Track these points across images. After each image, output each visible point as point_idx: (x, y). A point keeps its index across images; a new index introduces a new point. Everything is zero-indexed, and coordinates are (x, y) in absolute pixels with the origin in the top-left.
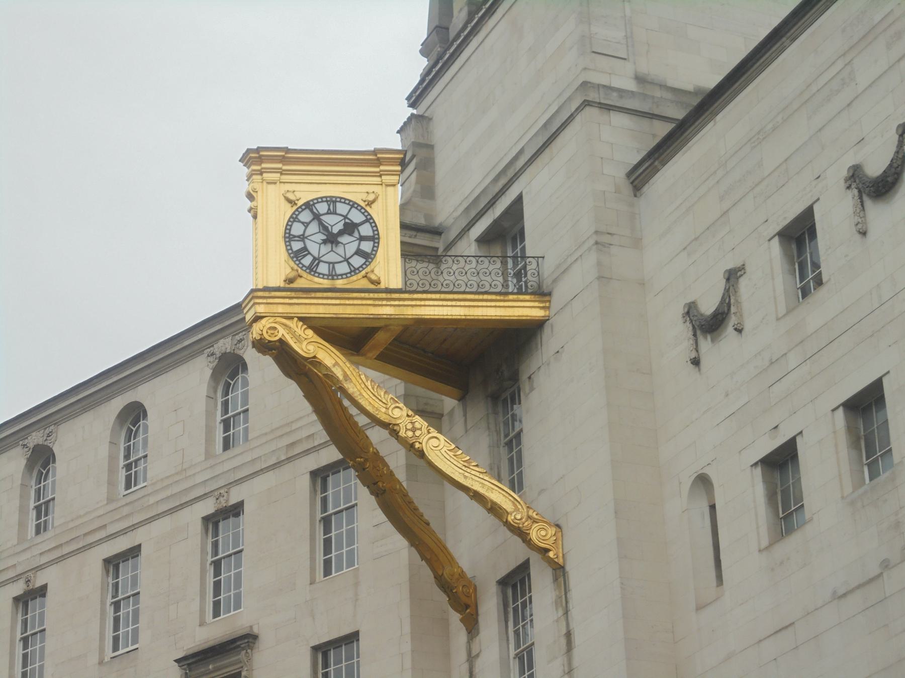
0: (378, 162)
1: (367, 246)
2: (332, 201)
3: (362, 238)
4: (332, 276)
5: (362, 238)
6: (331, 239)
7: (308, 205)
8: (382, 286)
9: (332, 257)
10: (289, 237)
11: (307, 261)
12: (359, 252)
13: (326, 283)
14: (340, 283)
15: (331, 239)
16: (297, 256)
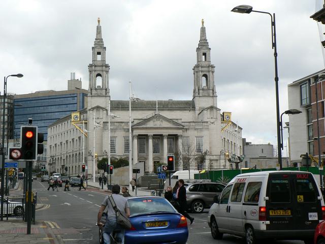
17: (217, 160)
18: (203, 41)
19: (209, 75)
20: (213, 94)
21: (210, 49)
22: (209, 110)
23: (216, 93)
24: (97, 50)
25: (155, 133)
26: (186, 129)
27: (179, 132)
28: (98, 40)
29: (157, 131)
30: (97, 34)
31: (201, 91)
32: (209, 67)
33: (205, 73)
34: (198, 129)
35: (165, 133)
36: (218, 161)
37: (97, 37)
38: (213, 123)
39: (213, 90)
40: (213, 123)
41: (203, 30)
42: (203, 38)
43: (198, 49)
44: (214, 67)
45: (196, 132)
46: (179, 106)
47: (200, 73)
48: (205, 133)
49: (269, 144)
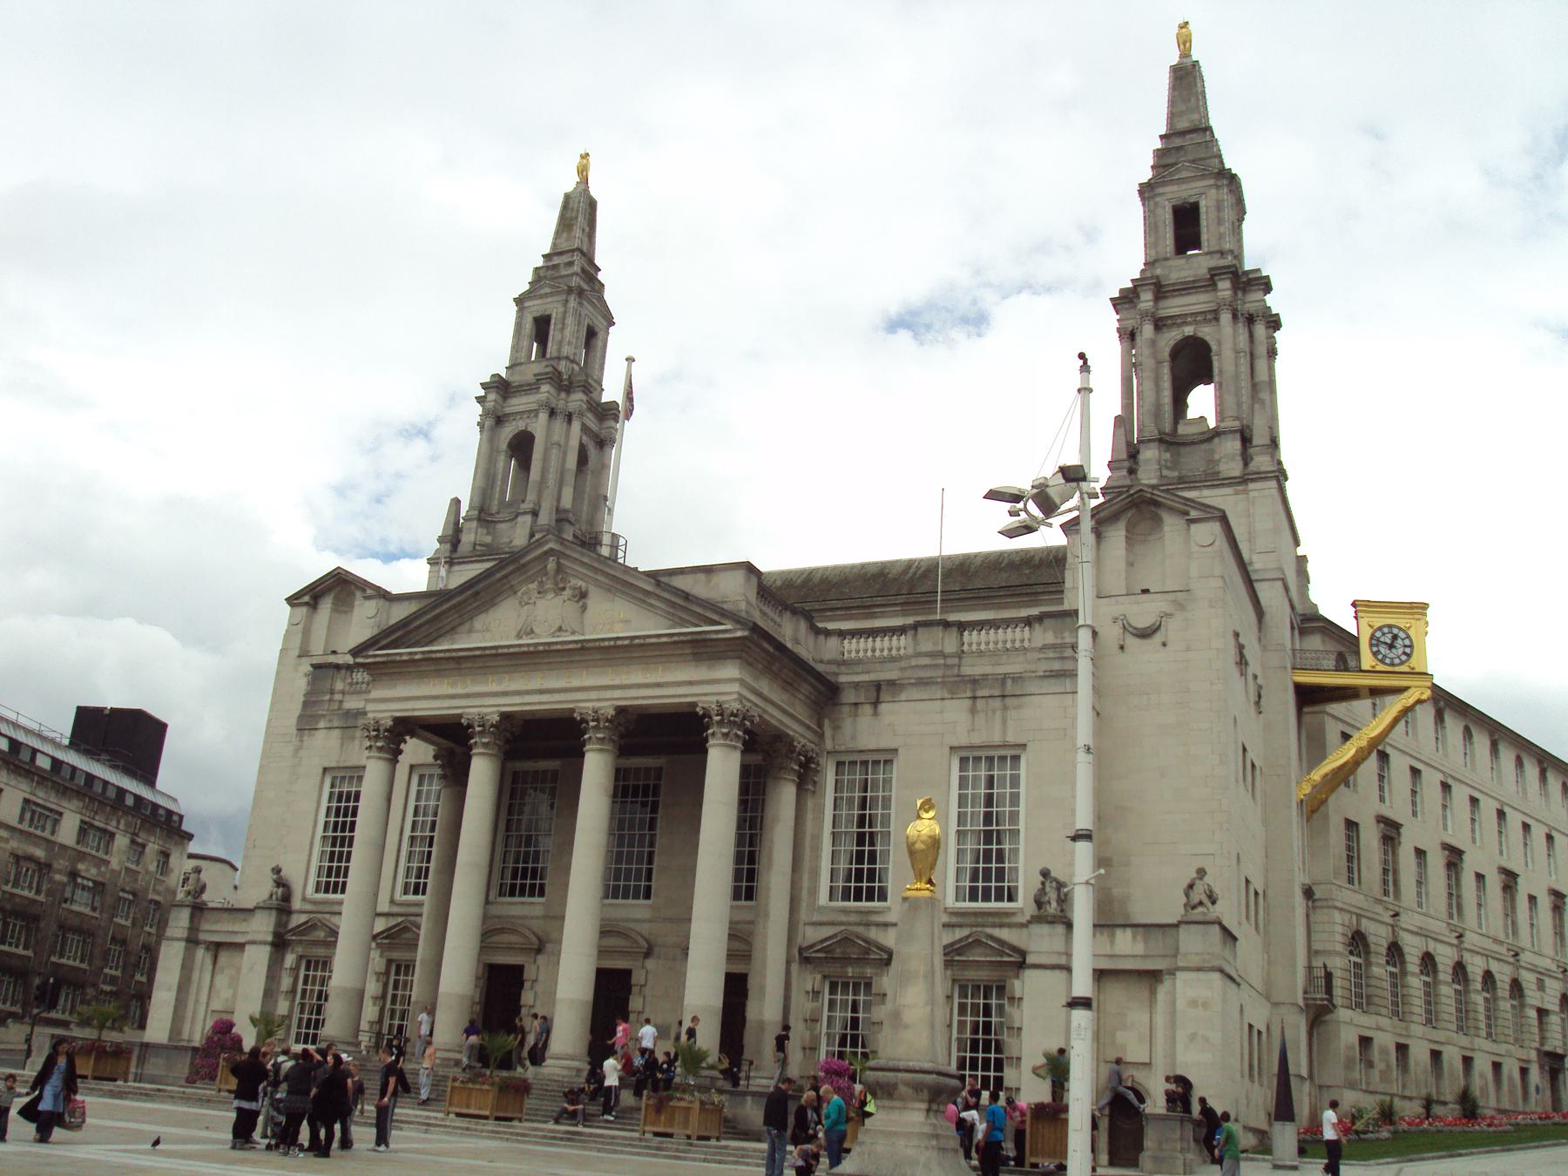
0: (1412, 608)
1: (1408, 650)
2: (1390, 626)
3: (1405, 646)
4: (1392, 664)
5: (1405, 646)
7: (1380, 629)
8: (1417, 670)
9: (1391, 655)
10: (1371, 645)
11: (1380, 657)
12: (1404, 653)
15: (1391, 646)
16: (1375, 654)
17: (1153, 977)
18: (1178, 142)
19: (1219, 343)
20: (1246, 459)
22: (1117, 535)
24: (536, 307)
25: (514, 704)
26: (878, 686)
28: (556, 260)
30: (558, 233)
33: (1188, 330)
34: (974, 682)
36: (1162, 991)
37: (554, 245)
38: (1145, 634)
40: (1145, 634)
41: (1186, 79)
42: (1183, 124)
46: (1003, 579)
47: (1148, 330)
49: (1141, 192)
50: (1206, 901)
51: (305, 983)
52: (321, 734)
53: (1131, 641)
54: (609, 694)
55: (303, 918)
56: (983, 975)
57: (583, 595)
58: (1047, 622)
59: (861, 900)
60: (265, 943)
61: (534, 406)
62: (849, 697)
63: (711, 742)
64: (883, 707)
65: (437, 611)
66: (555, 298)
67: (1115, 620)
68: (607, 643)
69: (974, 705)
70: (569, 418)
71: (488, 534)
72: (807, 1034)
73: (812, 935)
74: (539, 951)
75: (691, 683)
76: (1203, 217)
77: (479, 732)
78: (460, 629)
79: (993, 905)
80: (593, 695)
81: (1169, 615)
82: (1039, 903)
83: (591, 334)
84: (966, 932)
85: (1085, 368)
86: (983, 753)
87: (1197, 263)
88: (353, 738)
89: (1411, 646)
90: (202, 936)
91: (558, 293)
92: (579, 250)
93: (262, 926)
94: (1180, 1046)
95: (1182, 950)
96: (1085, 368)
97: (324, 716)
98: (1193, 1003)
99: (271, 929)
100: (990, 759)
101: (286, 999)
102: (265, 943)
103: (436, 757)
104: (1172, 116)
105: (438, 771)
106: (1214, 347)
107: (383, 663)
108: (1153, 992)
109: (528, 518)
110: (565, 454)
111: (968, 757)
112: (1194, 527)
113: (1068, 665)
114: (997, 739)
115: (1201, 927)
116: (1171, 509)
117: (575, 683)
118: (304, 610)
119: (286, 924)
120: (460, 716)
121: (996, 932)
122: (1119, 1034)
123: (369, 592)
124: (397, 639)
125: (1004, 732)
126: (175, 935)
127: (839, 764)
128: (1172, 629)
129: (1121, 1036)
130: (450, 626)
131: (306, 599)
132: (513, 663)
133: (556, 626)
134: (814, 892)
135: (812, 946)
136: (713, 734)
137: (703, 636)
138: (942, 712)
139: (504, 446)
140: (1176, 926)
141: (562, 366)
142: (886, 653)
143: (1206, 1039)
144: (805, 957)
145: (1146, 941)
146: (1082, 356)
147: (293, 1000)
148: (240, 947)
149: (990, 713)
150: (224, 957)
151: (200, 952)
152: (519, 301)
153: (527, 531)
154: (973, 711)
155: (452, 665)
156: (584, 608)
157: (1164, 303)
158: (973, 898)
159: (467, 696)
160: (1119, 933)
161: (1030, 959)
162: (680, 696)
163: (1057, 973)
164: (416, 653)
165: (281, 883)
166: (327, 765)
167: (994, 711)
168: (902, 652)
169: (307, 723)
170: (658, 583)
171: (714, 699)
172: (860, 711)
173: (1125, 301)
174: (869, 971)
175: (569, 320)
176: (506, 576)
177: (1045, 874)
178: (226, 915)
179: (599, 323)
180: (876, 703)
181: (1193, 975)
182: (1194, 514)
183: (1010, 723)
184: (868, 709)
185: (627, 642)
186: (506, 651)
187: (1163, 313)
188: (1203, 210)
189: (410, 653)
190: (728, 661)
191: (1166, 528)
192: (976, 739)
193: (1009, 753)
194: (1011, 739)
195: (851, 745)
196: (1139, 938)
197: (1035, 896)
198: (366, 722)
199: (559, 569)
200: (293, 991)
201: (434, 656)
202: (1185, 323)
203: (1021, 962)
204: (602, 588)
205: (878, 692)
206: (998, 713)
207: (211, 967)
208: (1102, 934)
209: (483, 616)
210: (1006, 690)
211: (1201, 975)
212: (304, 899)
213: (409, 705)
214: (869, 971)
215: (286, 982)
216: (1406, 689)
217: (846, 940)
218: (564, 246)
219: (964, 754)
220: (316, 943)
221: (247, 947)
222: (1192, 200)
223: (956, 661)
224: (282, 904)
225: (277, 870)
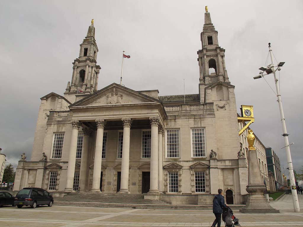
4: (248, 116)
6: (248, 113)
7: (246, 110)
13: (248, 117)
14: (249, 117)
16: (245, 114)
19: (218, 60)
21: (217, 32)
23: (228, 78)
24: (85, 47)
25: (107, 118)
26: (175, 116)
27: (155, 114)
28: (88, 38)
29: (112, 113)
31: (207, 78)
32: (216, 50)
33: (212, 58)
34: (195, 115)
35: (126, 115)
38: (222, 108)
39: (224, 77)
40: (222, 108)
41: (207, 15)
42: (208, 23)
43: (202, 34)
44: (224, 50)
45: (191, 121)
47: (205, 57)
48: (207, 122)
50: (243, 155)
51: (51, 177)
52: (52, 125)
53: (219, 109)
54: (129, 116)
55: (50, 163)
56: (201, 170)
57: (122, 96)
58: (207, 105)
59: (171, 157)
60: (42, 169)
61: (85, 65)
62: (169, 118)
63: (152, 125)
64: (176, 120)
65: (88, 99)
66: (89, 45)
67: (216, 105)
68: (129, 105)
69: (195, 120)
70: (92, 67)
71: (76, 89)
72: (165, 183)
73: (165, 164)
74: (106, 169)
75: (147, 113)
76: (213, 39)
77: (99, 123)
78: (93, 102)
79: (201, 157)
80: (125, 116)
81: (226, 104)
82: (211, 156)
83: (95, 52)
84: (196, 162)
85: (270, 46)
86: (196, 129)
87: (213, 47)
88: (60, 126)
89: (251, 113)
90: (26, 168)
91: (89, 44)
92: (92, 36)
93: (41, 165)
94: (241, 182)
95: (239, 164)
96: (270, 46)
97: (53, 122)
98: (242, 173)
99: (43, 166)
100: (198, 130)
101: (47, 180)
102: (42, 169)
103: (82, 130)
104: (205, 21)
105: (83, 132)
106: (216, 61)
107: (76, 109)
108: (233, 172)
109: (85, 86)
110: (91, 74)
111: (194, 129)
112: (229, 89)
113: (212, 113)
114: (200, 126)
115: (242, 160)
116: (224, 85)
117: (121, 113)
118: (45, 101)
119: (46, 165)
120: (95, 120)
121: (202, 162)
122: (227, 180)
123: (59, 97)
124: (79, 104)
125: (201, 125)
126: (20, 168)
127: (168, 131)
128: (227, 107)
129: (227, 180)
130: (91, 102)
131: (45, 98)
132: (106, 109)
133: (116, 102)
134: (165, 155)
135: (166, 166)
136: (153, 124)
137: (150, 104)
138: (188, 121)
139: (79, 72)
140: (238, 160)
141: (90, 57)
142: (175, 110)
143: (245, 180)
144: (164, 168)
145: (231, 163)
146: (269, 44)
147: (49, 181)
148: (36, 170)
149: (198, 121)
150: (31, 172)
151: (26, 172)
152: (81, 45)
153: (85, 88)
154: (194, 121)
155: (92, 109)
156: (122, 98)
157: (207, 53)
158: (196, 156)
159: (96, 116)
160: (226, 161)
161: (211, 167)
162: (145, 116)
163: (216, 169)
164: (84, 107)
165: (45, 156)
166: (54, 132)
167: (199, 121)
168: (178, 110)
169: (49, 124)
170: (140, 93)
171: (153, 117)
172: (172, 121)
173: (199, 52)
174: (177, 170)
175: (92, 49)
176: (104, 92)
177: (212, 151)
178: (32, 163)
179: (96, 51)
180: (175, 119)
181: (242, 168)
182: (229, 87)
183: (202, 123)
184: (173, 120)
185: (133, 105)
186: (105, 107)
187: (207, 54)
188: (213, 38)
189: (82, 107)
190: (155, 109)
191: (224, 89)
192: (196, 126)
193: (202, 129)
194: (202, 126)
195: (171, 127)
196: (230, 162)
197: (210, 155)
198: (72, 121)
199: (116, 91)
200: (48, 179)
201: (88, 107)
202: (211, 56)
203: (209, 168)
204: (126, 94)
205: (175, 118)
206: (200, 122)
207: (28, 174)
208: (223, 162)
209: (98, 100)
210: (201, 117)
211: (244, 168)
212: (50, 160)
213: (83, 118)
214: (177, 170)
215: (47, 177)
216: (250, 120)
217: (173, 164)
218: (89, 36)
219: (193, 129)
220: (53, 168)
221: (38, 170)
222: (211, 36)
223: (190, 112)
224: (45, 160)
225: (44, 153)
